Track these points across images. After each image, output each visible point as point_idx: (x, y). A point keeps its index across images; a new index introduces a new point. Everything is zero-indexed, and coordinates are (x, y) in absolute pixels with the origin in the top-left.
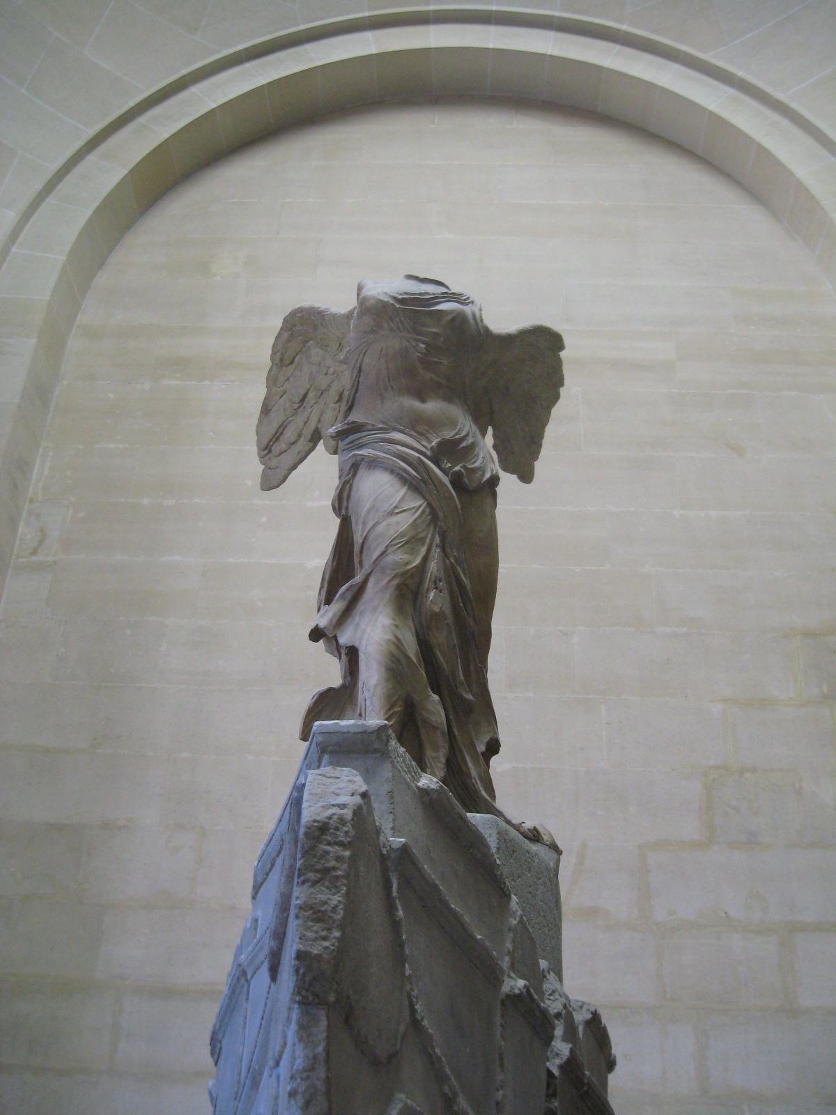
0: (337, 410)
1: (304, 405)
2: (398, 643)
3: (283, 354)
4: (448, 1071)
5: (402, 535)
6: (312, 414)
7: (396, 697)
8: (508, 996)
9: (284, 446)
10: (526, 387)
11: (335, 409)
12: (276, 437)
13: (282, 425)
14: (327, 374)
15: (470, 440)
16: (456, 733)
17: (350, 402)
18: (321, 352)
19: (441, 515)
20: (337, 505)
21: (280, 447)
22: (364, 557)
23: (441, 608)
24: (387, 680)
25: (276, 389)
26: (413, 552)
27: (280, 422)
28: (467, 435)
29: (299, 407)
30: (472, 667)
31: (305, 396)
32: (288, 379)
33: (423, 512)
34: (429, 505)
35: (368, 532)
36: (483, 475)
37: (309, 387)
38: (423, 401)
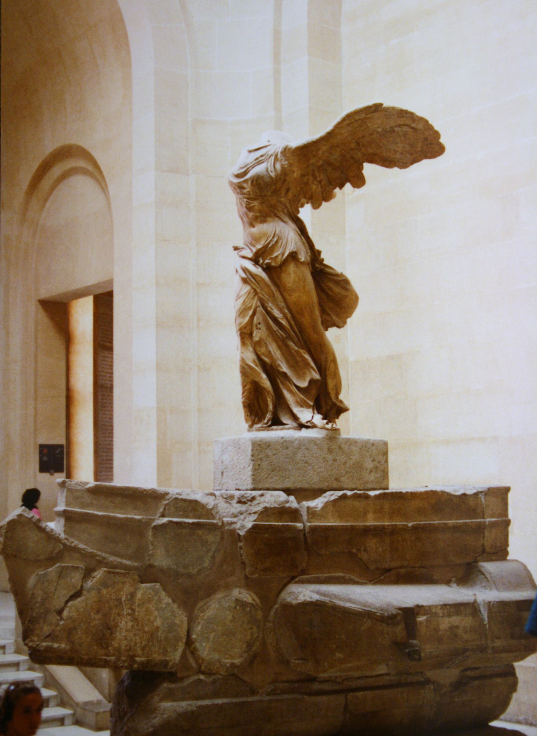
2: (243, 360)
4: (99, 553)
5: (239, 310)
7: (245, 384)
8: (155, 526)
10: (380, 130)
15: (275, 239)
16: (281, 386)
19: (258, 290)
23: (260, 337)
24: (242, 376)
26: (244, 317)
28: (273, 237)
30: (293, 351)
33: (249, 293)
34: (253, 288)
36: (283, 255)
38: (254, 226)
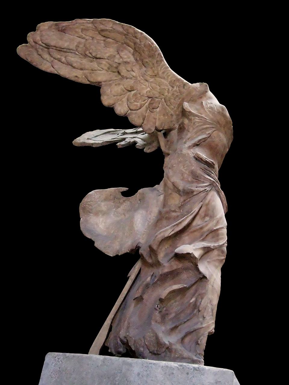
0: (124, 93)
1: (94, 59)
3: (107, 30)
6: (99, 72)
9: (63, 59)
11: (124, 91)
12: (60, 50)
13: (70, 50)
14: (129, 71)
17: (200, 142)
18: (132, 59)
20: (195, 193)
21: (59, 57)
22: (211, 235)
25: (80, 31)
27: (71, 47)
29: (90, 57)
31: (100, 58)
32: (93, 38)
35: (220, 228)
37: (106, 58)
